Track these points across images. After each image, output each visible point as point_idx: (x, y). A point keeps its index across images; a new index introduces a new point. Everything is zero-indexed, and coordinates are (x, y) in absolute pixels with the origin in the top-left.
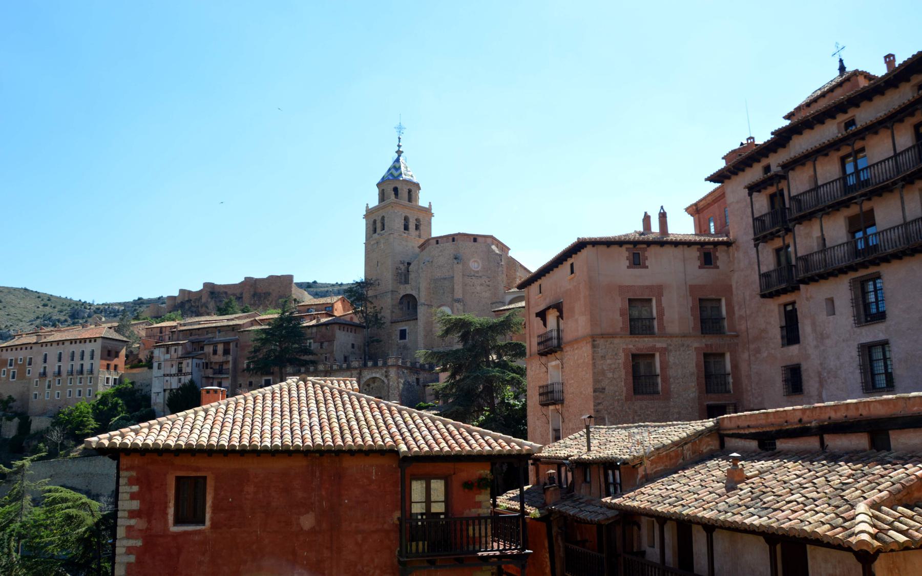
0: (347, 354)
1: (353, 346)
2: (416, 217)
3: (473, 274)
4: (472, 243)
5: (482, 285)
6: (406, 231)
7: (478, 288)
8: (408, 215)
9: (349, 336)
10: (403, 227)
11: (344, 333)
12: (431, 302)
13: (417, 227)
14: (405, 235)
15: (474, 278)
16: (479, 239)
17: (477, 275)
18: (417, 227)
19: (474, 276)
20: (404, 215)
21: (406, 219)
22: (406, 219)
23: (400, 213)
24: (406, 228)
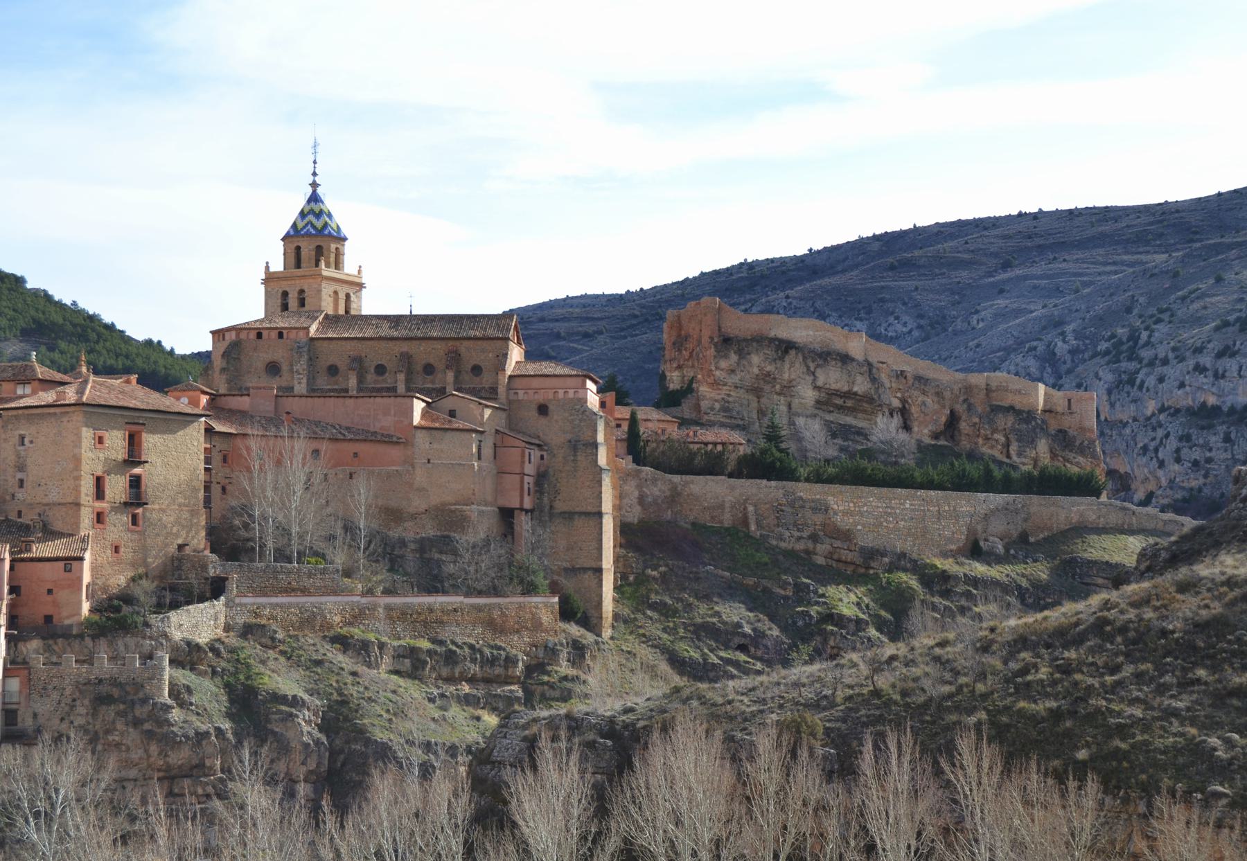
2: (298, 289)
8: (287, 289)
10: (279, 309)
20: (281, 291)
24: (285, 307)
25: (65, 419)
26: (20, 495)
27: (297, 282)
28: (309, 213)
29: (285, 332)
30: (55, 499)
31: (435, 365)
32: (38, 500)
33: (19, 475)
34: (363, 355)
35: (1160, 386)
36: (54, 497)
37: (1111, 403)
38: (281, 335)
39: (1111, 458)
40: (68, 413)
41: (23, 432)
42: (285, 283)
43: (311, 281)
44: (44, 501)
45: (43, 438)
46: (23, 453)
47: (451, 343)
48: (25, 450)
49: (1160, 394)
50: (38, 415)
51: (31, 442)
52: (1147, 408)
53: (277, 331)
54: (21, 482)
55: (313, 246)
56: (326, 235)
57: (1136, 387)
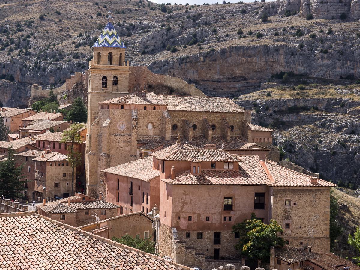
0: (57, 182)
1: (64, 175)
2: (113, 76)
3: (119, 133)
4: (119, 110)
5: (124, 141)
6: (104, 88)
7: (122, 144)
9: (60, 169)
11: (55, 167)
12: (97, 151)
13: (115, 83)
14: (103, 91)
15: (119, 136)
16: (125, 107)
17: (122, 134)
18: (115, 83)
19: (120, 135)
20: (102, 76)
21: (105, 78)
22: (105, 78)
23: (99, 75)
25: (319, 193)
26: (287, 232)
27: (113, 72)
28: (105, 34)
29: (157, 107)
30: (312, 235)
31: (216, 125)
32: (300, 235)
33: (286, 222)
34: (188, 119)
35: (58, 71)
36: (311, 233)
37: (22, 75)
38: (154, 108)
39: (24, 100)
40: (320, 190)
41: (289, 199)
42: (105, 72)
43: (122, 72)
44: (305, 236)
45: (303, 202)
46: (289, 210)
47: (223, 115)
48: (290, 208)
49: (58, 74)
50: (299, 190)
51: (295, 204)
52: (50, 80)
53: (153, 106)
54: (287, 226)
55: (119, 54)
56: (114, 48)
57: (41, 70)
